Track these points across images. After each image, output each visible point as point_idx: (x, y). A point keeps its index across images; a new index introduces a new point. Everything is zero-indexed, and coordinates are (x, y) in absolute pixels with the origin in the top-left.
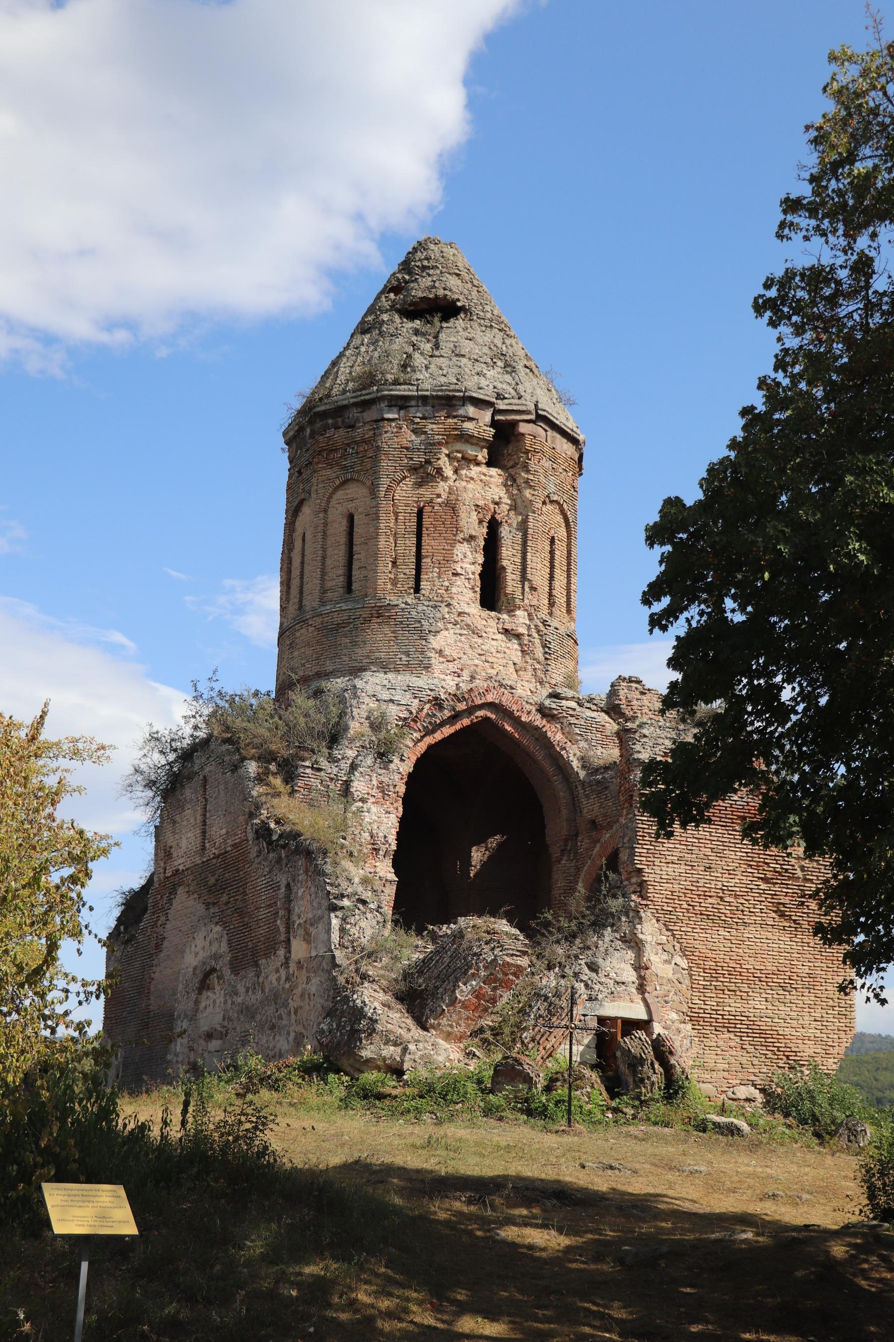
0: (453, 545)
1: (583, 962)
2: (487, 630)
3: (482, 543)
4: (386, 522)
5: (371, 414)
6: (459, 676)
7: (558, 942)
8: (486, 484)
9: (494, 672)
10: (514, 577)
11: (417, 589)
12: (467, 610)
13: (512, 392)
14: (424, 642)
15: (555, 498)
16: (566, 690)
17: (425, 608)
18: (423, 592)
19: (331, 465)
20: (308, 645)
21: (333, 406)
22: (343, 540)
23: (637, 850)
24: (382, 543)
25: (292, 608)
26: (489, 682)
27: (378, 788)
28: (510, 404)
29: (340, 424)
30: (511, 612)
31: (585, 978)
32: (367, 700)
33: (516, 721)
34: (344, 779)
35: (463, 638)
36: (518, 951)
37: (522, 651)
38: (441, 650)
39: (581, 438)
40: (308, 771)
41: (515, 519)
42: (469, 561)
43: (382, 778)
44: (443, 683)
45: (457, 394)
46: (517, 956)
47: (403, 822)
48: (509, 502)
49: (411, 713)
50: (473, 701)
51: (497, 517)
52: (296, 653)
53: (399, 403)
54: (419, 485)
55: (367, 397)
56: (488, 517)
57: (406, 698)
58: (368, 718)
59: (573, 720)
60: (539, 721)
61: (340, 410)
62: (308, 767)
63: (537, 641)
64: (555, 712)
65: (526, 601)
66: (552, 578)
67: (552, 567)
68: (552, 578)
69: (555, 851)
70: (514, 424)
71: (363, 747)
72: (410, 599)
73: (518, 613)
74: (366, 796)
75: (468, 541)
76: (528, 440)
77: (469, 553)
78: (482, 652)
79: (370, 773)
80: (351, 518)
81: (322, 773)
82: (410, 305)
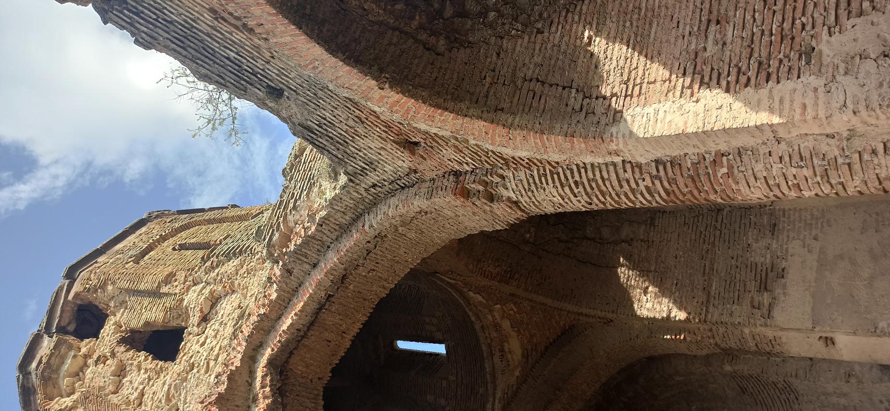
63: (222, 269)
65: (177, 291)
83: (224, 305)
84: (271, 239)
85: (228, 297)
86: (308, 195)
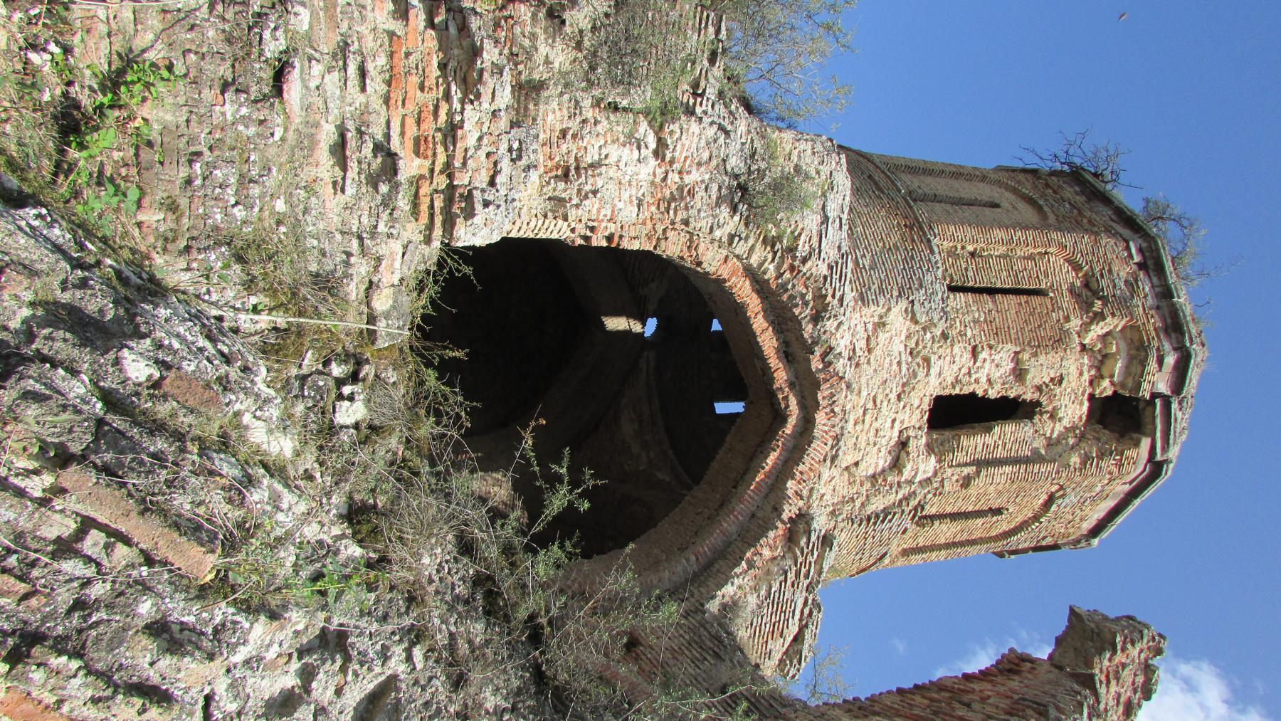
0: (1016, 342)
1: (397, 665)
2: (907, 408)
3: (1012, 394)
4: (1026, 243)
6: (849, 359)
7: (466, 547)
10: (979, 448)
11: (953, 289)
12: (932, 371)
14: (895, 293)
18: (952, 296)
24: (999, 234)
26: (841, 416)
27: (680, 189)
30: (930, 448)
31: (322, 689)
32: (825, 170)
33: (785, 470)
34: (698, 110)
35: (895, 367)
37: (874, 476)
38: (884, 325)
39: (1095, 542)
40: (711, 30)
41: (1039, 444)
42: (990, 376)
44: (845, 327)
48: (1055, 436)
49: (804, 260)
50: (826, 381)
51: (1037, 418)
53: (1150, 263)
54: (1072, 291)
56: (1044, 400)
57: (830, 252)
58: (797, 169)
59: (791, 576)
60: (789, 512)
62: (718, 32)
63: (892, 498)
64: (803, 542)
65: (949, 471)
66: (955, 516)
68: (955, 516)
71: (753, 155)
73: (933, 459)
74: (669, 156)
75: (1014, 369)
77: (1002, 371)
78: (878, 402)
79: (714, 163)
81: (706, 63)
84: (809, 539)
85: (879, 470)
86: (771, 588)
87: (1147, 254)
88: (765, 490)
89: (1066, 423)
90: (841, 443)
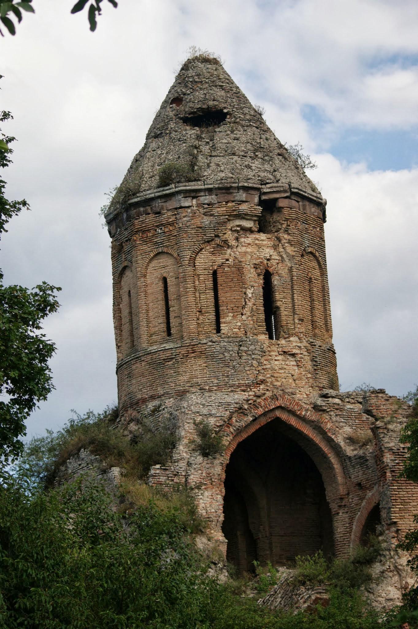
5: (172, 204)
8: (259, 247)
9: (278, 384)
10: (286, 313)
11: (218, 330)
13: (271, 177)
15: (310, 250)
16: (331, 391)
17: (225, 344)
18: (222, 332)
19: (145, 241)
20: (143, 375)
21: (143, 198)
22: (161, 296)
23: (392, 509)
25: (125, 347)
28: (271, 187)
29: (149, 211)
34: (184, 474)
36: (323, 590)
43: (209, 471)
45: (233, 185)
46: (323, 593)
47: (225, 499)
49: (225, 421)
51: (271, 270)
52: (134, 381)
53: (192, 195)
54: (213, 253)
55: (167, 192)
61: (148, 202)
64: (324, 408)
65: (297, 330)
66: (312, 308)
67: (312, 301)
68: (312, 308)
69: (334, 506)
70: (276, 200)
72: (215, 338)
76: (286, 211)
80: (165, 280)
81: (167, 472)
82: (189, 114)
83: (292, 363)
85: (295, 363)
87: (188, 195)
88: (304, 423)
89: (272, 252)
90: (287, 391)
